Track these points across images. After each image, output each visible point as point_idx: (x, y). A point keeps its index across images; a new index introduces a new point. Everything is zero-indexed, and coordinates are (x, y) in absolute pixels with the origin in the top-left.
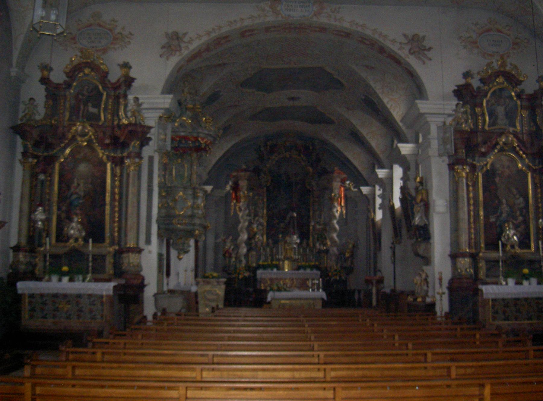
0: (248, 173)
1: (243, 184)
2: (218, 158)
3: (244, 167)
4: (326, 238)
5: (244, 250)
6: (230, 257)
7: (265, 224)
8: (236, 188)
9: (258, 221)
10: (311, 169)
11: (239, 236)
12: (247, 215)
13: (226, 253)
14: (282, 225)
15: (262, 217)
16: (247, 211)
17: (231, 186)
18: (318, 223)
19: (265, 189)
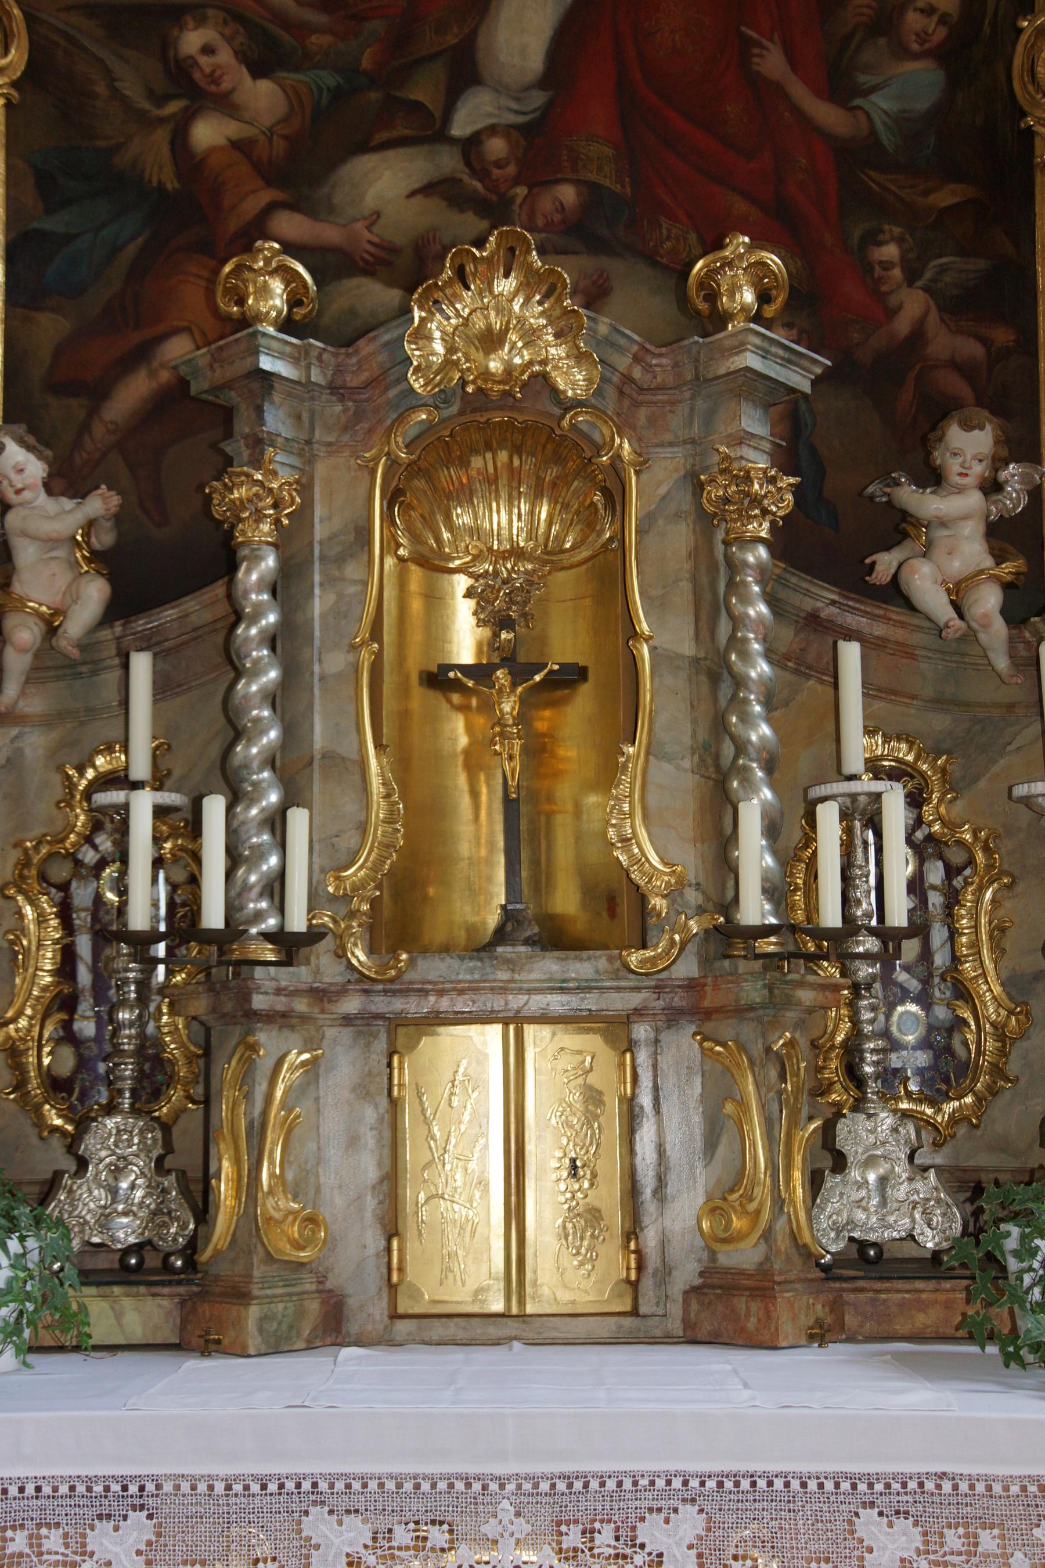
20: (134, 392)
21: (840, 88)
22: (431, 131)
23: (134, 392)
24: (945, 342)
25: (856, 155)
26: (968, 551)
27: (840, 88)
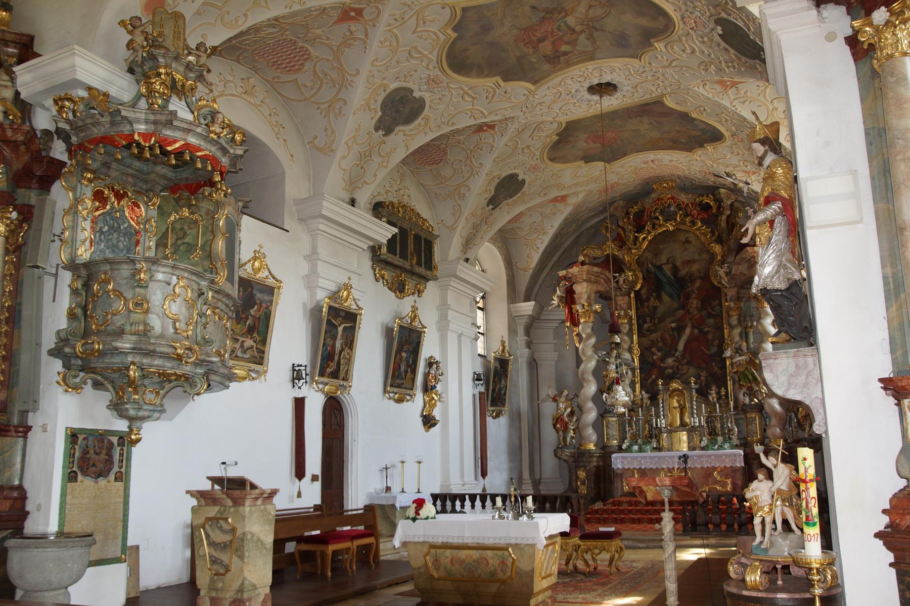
0: (585, 267)
1: (582, 290)
2: (541, 251)
3: (581, 258)
4: (758, 383)
5: (591, 415)
6: (566, 429)
7: (637, 363)
8: (569, 298)
9: (618, 356)
10: (717, 249)
11: (582, 387)
12: (596, 348)
13: (557, 421)
14: (670, 361)
15: (630, 350)
16: (593, 341)
17: (561, 298)
18: (738, 351)
19: (632, 295)
20: (650, 380)
21: (709, 350)
22: (674, 356)
23: (650, 380)
24: (719, 372)
25: (711, 355)
26: (714, 395)
27: (709, 350)
